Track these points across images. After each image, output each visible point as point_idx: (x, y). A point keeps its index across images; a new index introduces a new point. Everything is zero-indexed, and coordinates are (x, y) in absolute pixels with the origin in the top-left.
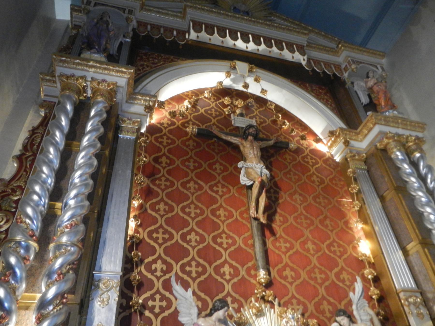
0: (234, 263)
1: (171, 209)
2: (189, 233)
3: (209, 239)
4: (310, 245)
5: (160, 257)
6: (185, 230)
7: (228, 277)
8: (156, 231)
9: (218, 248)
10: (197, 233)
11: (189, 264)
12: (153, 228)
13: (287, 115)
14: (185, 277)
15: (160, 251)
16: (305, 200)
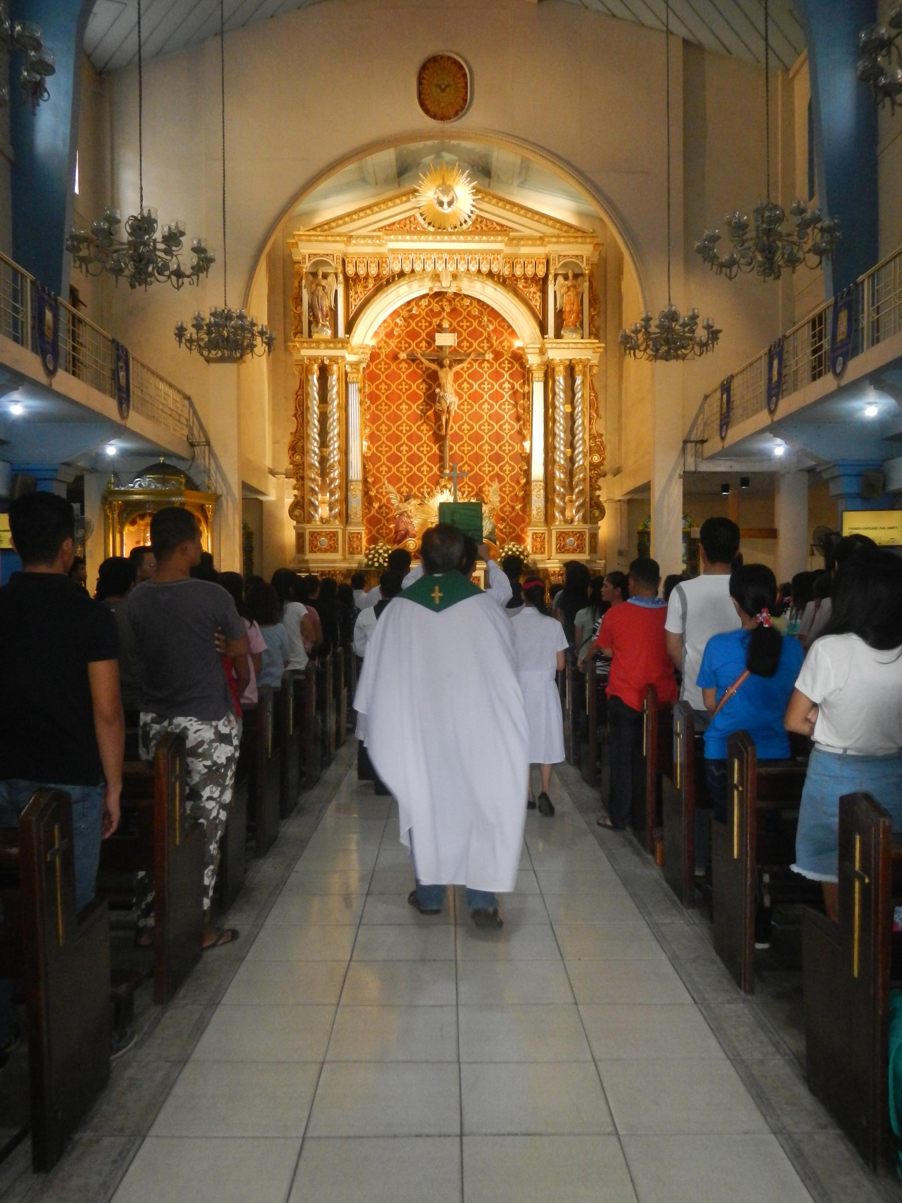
0: (430, 464)
1: (390, 428)
2: (402, 445)
3: (415, 449)
4: (486, 447)
5: (384, 463)
6: (399, 443)
7: (425, 473)
8: (381, 446)
9: (420, 454)
10: (407, 445)
11: (401, 466)
12: (378, 444)
13: (494, 314)
14: (399, 475)
15: (384, 459)
16: (492, 407)
